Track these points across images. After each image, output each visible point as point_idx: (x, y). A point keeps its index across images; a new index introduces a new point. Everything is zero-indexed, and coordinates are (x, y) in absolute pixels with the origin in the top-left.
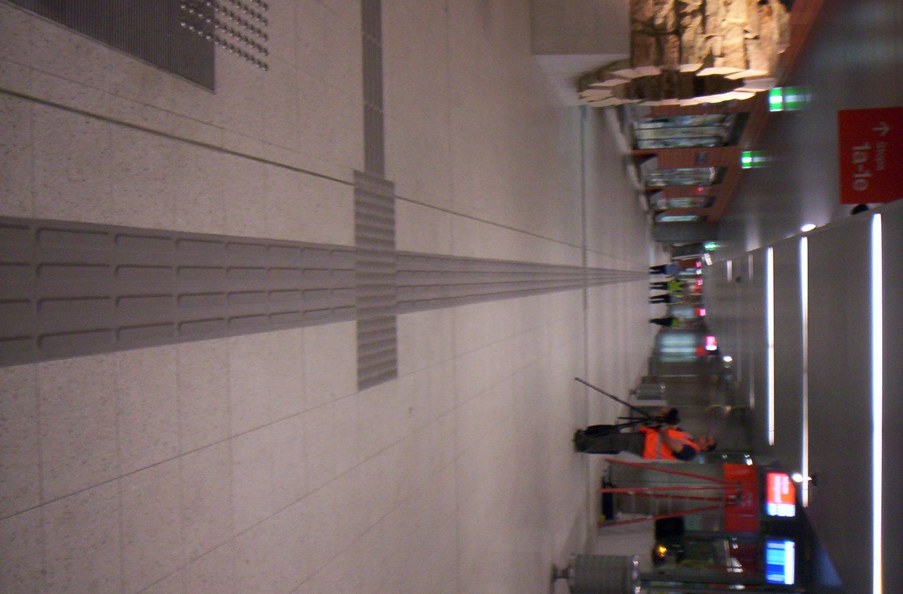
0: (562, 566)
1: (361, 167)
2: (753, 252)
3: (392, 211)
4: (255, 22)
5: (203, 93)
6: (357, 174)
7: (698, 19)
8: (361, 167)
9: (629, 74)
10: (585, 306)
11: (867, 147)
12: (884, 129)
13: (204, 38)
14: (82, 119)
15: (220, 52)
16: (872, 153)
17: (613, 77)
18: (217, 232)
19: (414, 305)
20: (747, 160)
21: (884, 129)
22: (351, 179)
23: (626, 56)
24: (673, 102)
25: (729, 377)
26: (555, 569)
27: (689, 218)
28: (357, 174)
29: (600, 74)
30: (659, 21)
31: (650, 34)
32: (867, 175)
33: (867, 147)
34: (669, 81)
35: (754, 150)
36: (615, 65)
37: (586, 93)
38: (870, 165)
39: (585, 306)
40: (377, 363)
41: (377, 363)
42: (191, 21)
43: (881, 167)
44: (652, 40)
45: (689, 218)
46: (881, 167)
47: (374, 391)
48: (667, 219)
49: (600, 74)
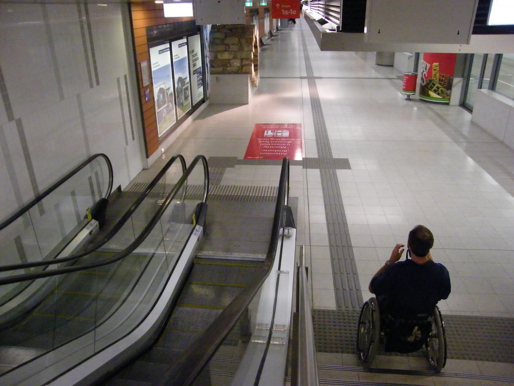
1: (302, 167)
6: (303, 168)
7: (238, 53)
10: (320, 78)
11: (283, 10)
12: (278, 5)
16: (285, 9)
19: (330, 153)
20: (264, 4)
21: (278, 5)
26: (407, 99)
28: (303, 168)
29: (253, 82)
30: (239, 65)
31: (242, 67)
32: (291, 10)
33: (283, 10)
36: (251, 78)
38: (288, 9)
39: (320, 78)
40: (345, 164)
41: (345, 164)
43: (289, 6)
44: (244, 68)
46: (289, 6)
48: (279, 24)
49: (253, 82)
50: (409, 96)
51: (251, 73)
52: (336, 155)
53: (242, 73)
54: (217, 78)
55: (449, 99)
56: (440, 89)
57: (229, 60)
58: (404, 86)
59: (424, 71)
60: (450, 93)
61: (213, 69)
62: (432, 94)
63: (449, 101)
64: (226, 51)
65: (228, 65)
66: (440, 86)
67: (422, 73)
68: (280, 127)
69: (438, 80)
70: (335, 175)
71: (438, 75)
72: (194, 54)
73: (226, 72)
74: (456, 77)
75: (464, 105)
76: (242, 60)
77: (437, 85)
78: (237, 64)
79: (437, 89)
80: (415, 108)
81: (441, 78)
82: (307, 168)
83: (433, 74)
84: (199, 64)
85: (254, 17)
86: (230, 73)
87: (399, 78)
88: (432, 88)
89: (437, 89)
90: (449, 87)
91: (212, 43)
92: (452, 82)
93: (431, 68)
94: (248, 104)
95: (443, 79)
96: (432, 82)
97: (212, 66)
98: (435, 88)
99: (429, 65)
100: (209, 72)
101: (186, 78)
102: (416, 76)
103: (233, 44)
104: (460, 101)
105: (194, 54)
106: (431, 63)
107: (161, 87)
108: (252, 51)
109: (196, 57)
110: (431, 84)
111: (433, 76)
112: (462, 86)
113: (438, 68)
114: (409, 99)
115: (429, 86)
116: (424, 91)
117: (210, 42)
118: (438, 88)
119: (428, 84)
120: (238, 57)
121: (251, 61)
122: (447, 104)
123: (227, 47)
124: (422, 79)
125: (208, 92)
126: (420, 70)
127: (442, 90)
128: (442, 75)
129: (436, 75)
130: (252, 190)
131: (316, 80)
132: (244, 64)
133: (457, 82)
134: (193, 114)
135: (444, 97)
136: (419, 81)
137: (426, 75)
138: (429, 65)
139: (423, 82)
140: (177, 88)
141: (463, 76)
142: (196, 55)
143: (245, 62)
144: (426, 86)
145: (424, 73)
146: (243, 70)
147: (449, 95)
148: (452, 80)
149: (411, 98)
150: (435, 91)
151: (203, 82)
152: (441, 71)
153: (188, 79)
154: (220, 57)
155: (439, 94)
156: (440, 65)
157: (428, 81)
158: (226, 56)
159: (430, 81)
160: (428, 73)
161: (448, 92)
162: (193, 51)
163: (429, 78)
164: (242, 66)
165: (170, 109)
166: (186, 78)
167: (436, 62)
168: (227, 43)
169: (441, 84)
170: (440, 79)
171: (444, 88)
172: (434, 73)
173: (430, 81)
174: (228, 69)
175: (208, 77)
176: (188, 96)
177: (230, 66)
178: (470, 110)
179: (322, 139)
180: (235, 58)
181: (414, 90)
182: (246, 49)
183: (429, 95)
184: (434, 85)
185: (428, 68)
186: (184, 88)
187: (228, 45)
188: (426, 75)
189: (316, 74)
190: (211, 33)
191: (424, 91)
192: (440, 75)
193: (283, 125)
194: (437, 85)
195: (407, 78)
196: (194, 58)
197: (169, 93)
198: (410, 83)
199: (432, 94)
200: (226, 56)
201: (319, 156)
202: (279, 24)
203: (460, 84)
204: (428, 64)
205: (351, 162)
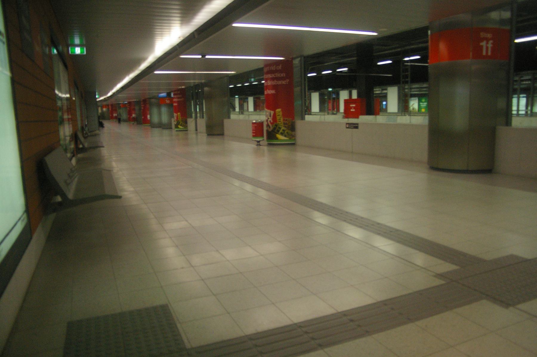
0: (256, 143)
26: (257, 145)
50: (259, 142)
58: (253, 133)
71: (282, 119)
77: (283, 128)
88: (278, 131)
93: (275, 115)
98: (281, 131)
99: (272, 112)
106: (274, 109)
110: (277, 128)
113: (281, 113)
115: (276, 131)
116: (271, 136)
118: (284, 130)
119: (275, 129)
122: (294, 144)
124: (268, 125)
129: (280, 119)
135: (290, 138)
136: (265, 128)
138: (272, 112)
139: (270, 127)
144: (272, 131)
145: (269, 120)
150: (282, 134)
152: (284, 115)
155: (285, 136)
156: (282, 110)
160: (273, 119)
161: (293, 133)
167: (278, 108)
169: (286, 127)
170: (284, 124)
172: (278, 118)
173: (276, 126)
181: (262, 135)
183: (277, 139)
184: (280, 128)
185: (272, 114)
191: (271, 136)
192: (284, 120)
194: (283, 128)
199: (279, 136)
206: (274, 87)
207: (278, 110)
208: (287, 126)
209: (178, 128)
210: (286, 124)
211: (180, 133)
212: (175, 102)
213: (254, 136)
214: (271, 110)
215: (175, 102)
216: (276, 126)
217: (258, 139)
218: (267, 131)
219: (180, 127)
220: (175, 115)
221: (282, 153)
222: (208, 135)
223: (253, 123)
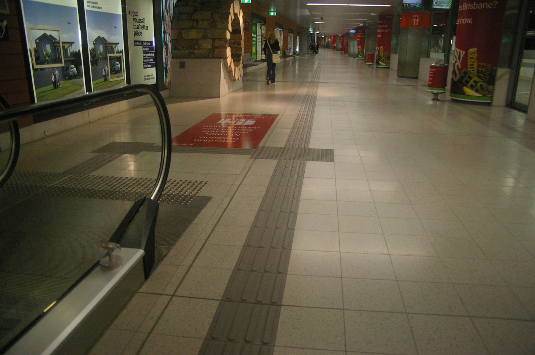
0: (432, 96)
1: (250, 156)
2: (310, 11)
3: (268, 147)
4: (191, 184)
5: (212, 199)
6: (251, 158)
8: (250, 156)
9: (229, 60)
13: (194, 199)
14: (214, 232)
15: (198, 194)
17: (230, 66)
18: (261, 199)
20: (272, 14)
22: (253, 160)
23: (222, 60)
24: (242, 42)
25: (367, 25)
26: (433, 99)
27: (298, 40)
29: (229, 71)
30: (210, 47)
31: (214, 51)
34: (234, 44)
35: (269, 11)
37: (236, 77)
40: (326, 155)
42: (188, 202)
44: (216, 50)
45: (298, 40)
47: (336, 157)
48: (297, 50)
49: (229, 71)
50: (436, 94)
51: (226, 58)
52: (315, 144)
53: (213, 57)
54: (180, 63)
55: (492, 97)
56: (479, 84)
57: (197, 40)
59: (456, 62)
60: (493, 90)
61: (176, 52)
62: (468, 90)
63: (492, 100)
64: (193, 28)
65: (196, 48)
66: (479, 80)
67: (454, 65)
68: (247, 116)
69: (476, 71)
70: (302, 169)
71: (476, 65)
72: (135, 17)
73: (193, 55)
74: (501, 67)
75: (512, 104)
76: (214, 40)
77: (475, 78)
78: (207, 45)
79: (474, 84)
80: (446, 107)
81: (480, 69)
82: (257, 157)
83: (469, 63)
84: (149, 35)
85: (258, 24)
86: (196, 57)
87: (424, 86)
88: (467, 82)
89: (474, 84)
90: (492, 81)
91: (176, 18)
92: (495, 75)
93: (466, 56)
94: (219, 97)
95: (483, 70)
96: (468, 75)
97: (174, 48)
98: (471, 82)
100: (170, 55)
101: (117, 44)
102: (446, 69)
103: (203, 20)
104: (507, 101)
105: (135, 17)
106: (466, 50)
107: (49, 33)
108: (227, 28)
109: (142, 24)
110: (466, 78)
111: (469, 66)
112: (510, 80)
113: (475, 56)
114: (435, 99)
115: (464, 81)
116: (457, 89)
117: (174, 17)
118: (476, 82)
119: (462, 78)
120: (209, 36)
121: (225, 40)
122: (489, 104)
123: (195, 23)
124: (454, 72)
125: (167, 80)
126: (452, 60)
127: (481, 86)
128: (482, 64)
129: (473, 64)
130: (143, 183)
131: (320, 84)
132: (216, 45)
133: (503, 74)
134: (131, 100)
135: (484, 95)
137: (460, 67)
139: (456, 76)
140: (93, 50)
141: (510, 66)
142: (143, 21)
143: (218, 43)
144: (458, 81)
146: (216, 54)
147: (492, 92)
148: (495, 71)
149: (439, 98)
150: (472, 87)
151: (157, 63)
152: (479, 59)
153: (121, 47)
154: (185, 36)
155: (477, 91)
157: (462, 74)
158: (193, 34)
159: (465, 73)
161: (490, 88)
162: (135, 14)
163: (464, 70)
164: (214, 48)
165: (71, 73)
166: (117, 44)
168: (196, 18)
169: (480, 77)
171: (484, 82)
172: (470, 62)
174: (196, 52)
175: (167, 59)
176: (120, 71)
177: (199, 48)
178: (523, 109)
179: (303, 128)
180: (204, 37)
182: (219, 27)
183: (464, 93)
184: (471, 78)
185: (462, 56)
186: (109, 55)
187: (196, 21)
188: (460, 67)
189: (320, 81)
190: (176, 7)
191: (457, 89)
192: (479, 66)
193: (251, 115)
194: (475, 78)
195: (434, 70)
196: (137, 24)
197: (70, 50)
198: (438, 77)
199: (468, 90)
200: (193, 34)
201: (286, 145)
202: (297, 50)
203: (507, 77)
204: (461, 51)
205: (336, 153)
206: (471, 14)
207: (471, 50)
208: (482, 75)
209: (379, 64)
210: (481, 72)
211: (381, 70)
212: (378, 33)
213: (430, 86)
214: (461, 49)
215: (378, 33)
216: (465, 73)
217: (435, 91)
218: (452, 80)
219: (380, 62)
220: (377, 48)
221: (467, 117)
222: (399, 76)
223: (432, 67)
